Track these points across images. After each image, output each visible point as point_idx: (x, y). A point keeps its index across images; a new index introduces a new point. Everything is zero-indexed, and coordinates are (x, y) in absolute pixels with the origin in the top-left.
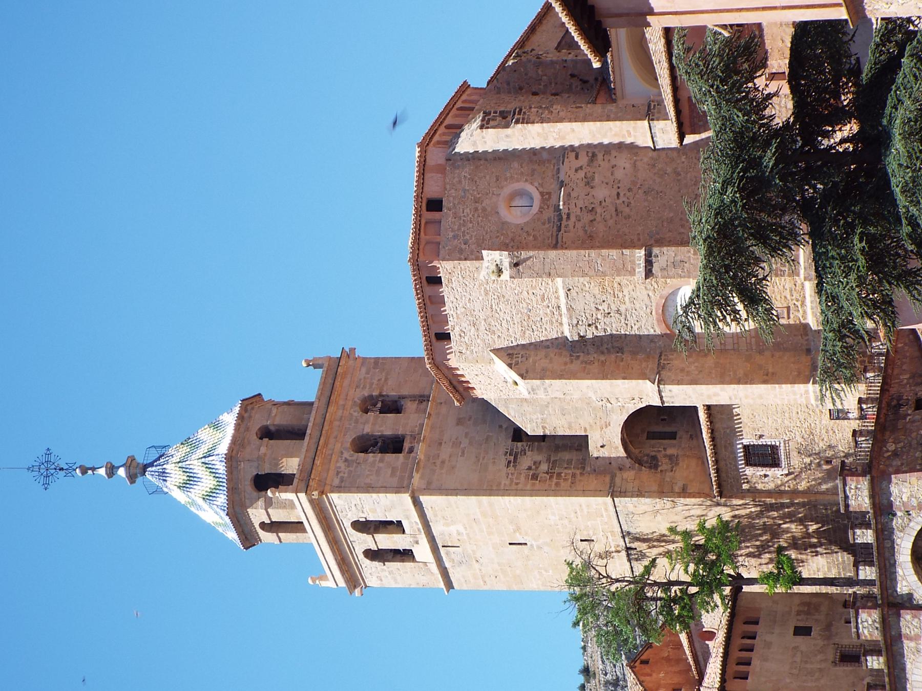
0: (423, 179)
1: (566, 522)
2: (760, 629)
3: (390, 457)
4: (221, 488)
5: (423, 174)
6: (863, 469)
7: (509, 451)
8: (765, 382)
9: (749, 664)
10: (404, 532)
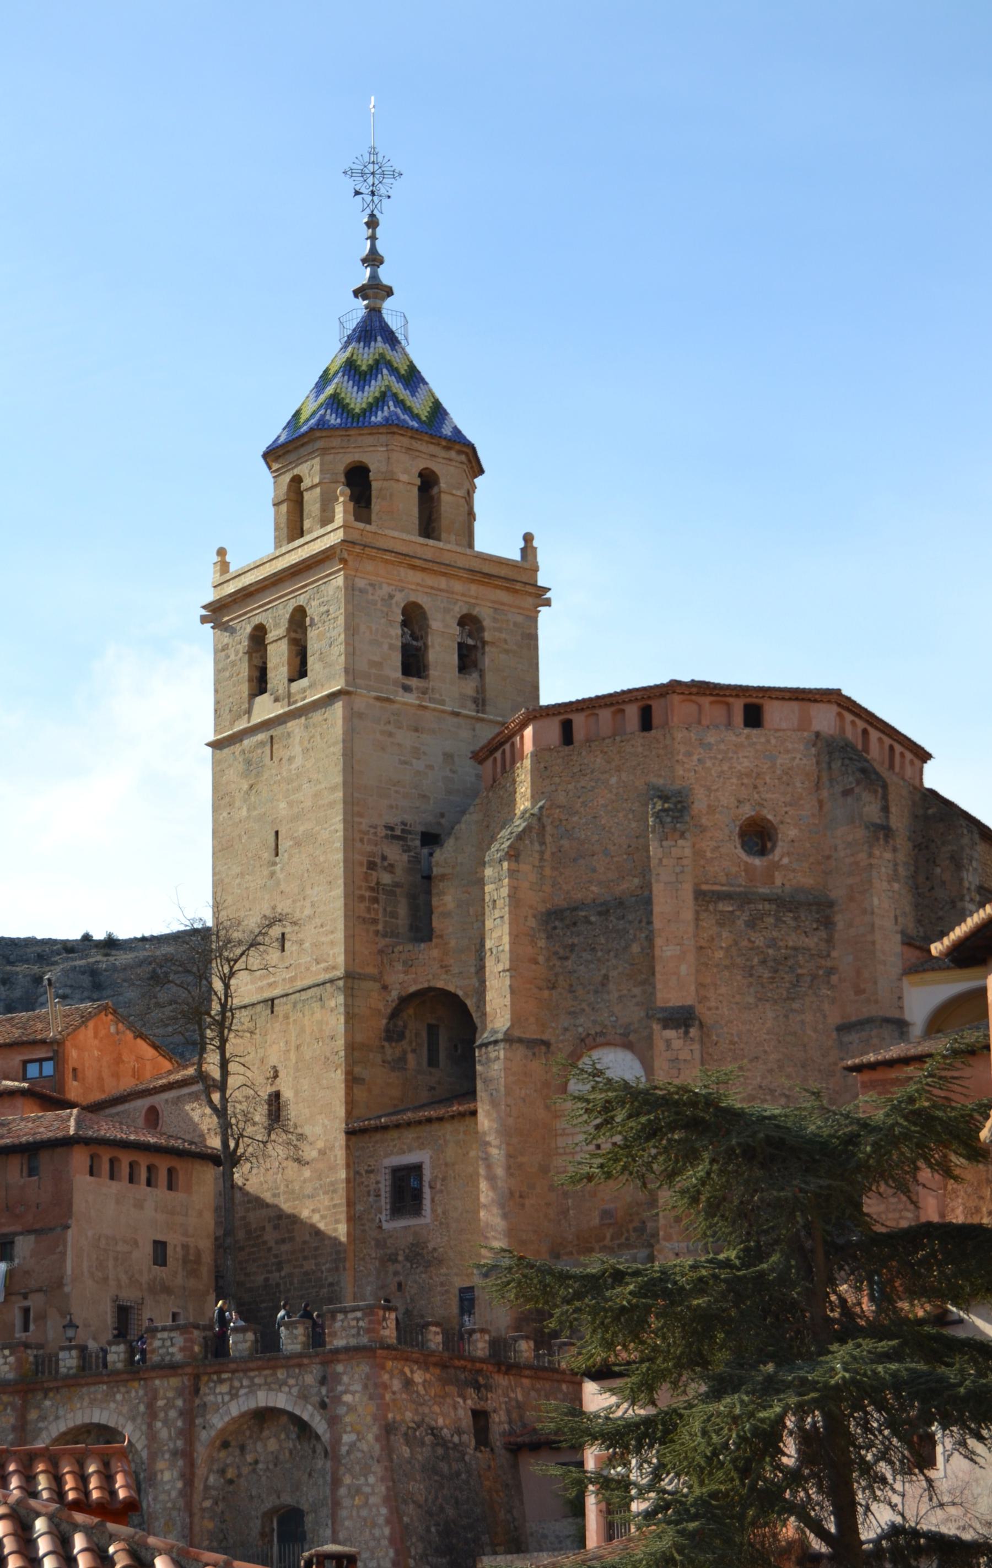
0: (790, 699)
1: (308, 911)
2: (161, 1192)
3: (397, 659)
4: (350, 420)
5: (797, 699)
6: (386, 1337)
7: (407, 828)
8: (512, 1194)
9: (112, 1177)
10: (291, 680)
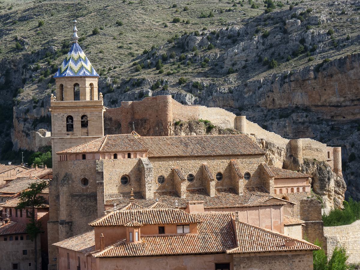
3: (65, 129)
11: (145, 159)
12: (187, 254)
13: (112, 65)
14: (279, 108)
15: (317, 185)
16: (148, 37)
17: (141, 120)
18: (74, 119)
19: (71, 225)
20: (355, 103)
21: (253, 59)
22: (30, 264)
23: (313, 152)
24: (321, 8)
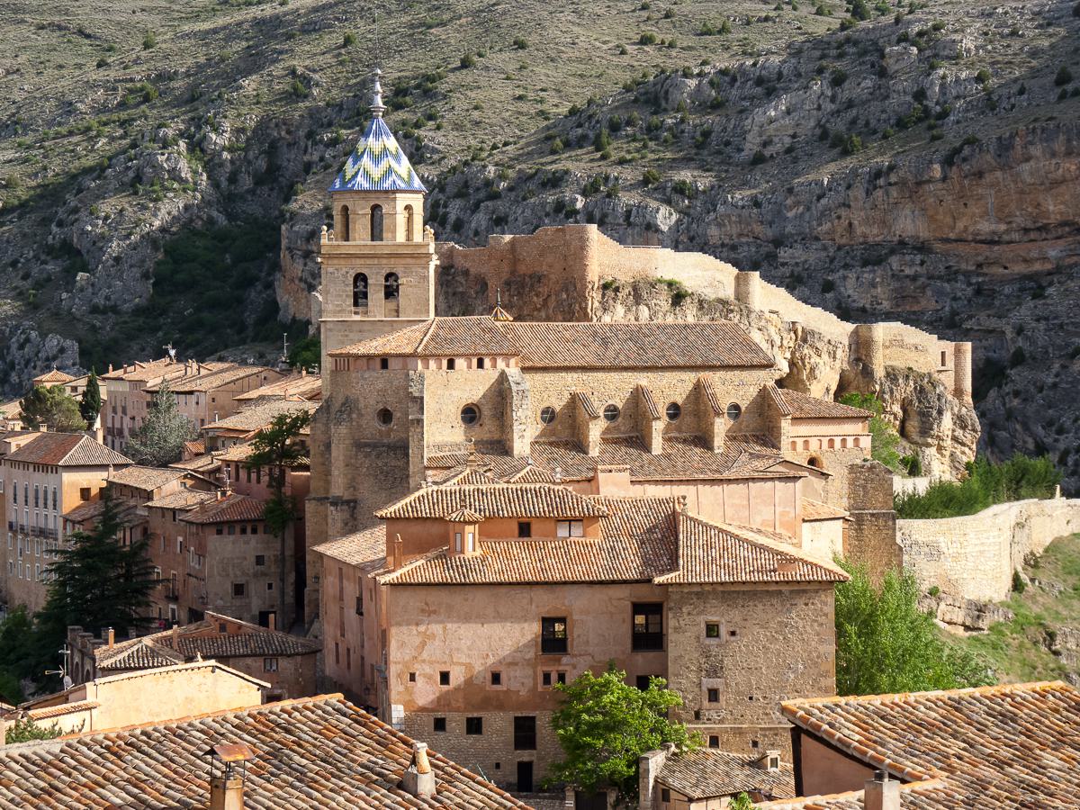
11: (513, 371)
12: (574, 583)
13: (499, 137)
14: (861, 244)
15: (913, 426)
16: (581, 76)
17: (530, 277)
18: (370, 281)
19: (355, 508)
20: (1032, 235)
21: (810, 133)
22: (270, 586)
23: (907, 351)
24: (965, 22)
